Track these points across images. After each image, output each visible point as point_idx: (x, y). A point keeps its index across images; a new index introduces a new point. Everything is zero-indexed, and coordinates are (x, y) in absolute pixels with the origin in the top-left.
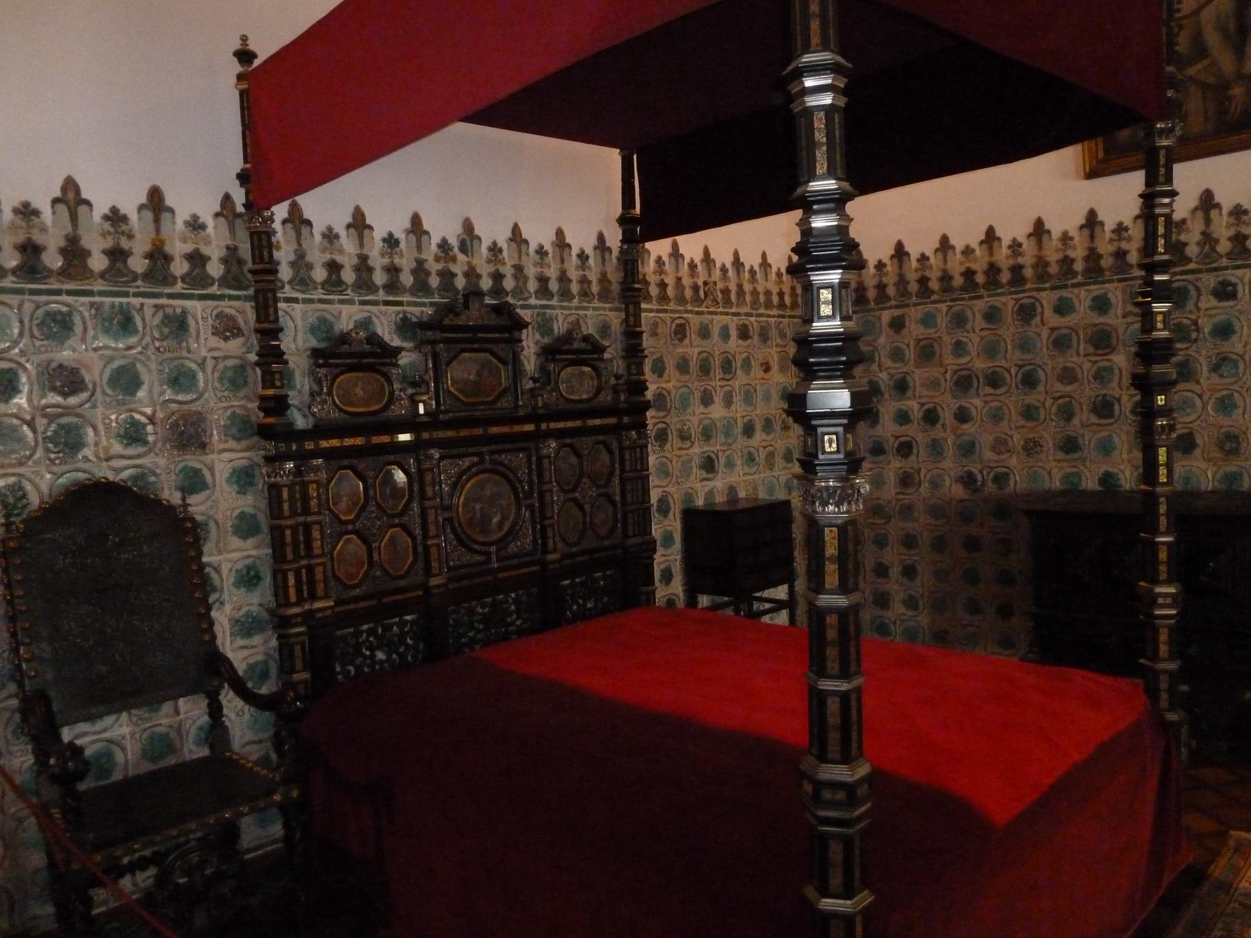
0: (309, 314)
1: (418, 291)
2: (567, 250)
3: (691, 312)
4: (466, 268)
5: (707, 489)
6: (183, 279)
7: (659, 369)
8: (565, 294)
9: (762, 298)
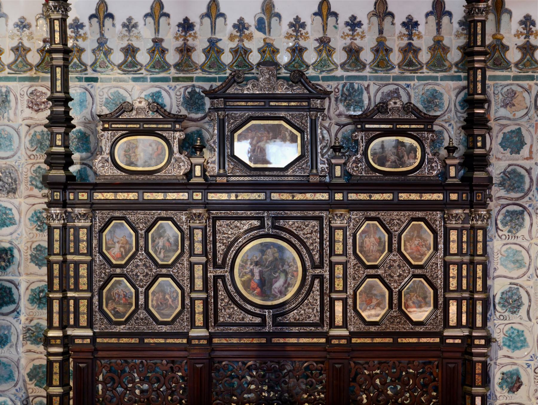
0: (105, 90)
1: (210, 67)
2: (388, 19)
4: (262, 44)
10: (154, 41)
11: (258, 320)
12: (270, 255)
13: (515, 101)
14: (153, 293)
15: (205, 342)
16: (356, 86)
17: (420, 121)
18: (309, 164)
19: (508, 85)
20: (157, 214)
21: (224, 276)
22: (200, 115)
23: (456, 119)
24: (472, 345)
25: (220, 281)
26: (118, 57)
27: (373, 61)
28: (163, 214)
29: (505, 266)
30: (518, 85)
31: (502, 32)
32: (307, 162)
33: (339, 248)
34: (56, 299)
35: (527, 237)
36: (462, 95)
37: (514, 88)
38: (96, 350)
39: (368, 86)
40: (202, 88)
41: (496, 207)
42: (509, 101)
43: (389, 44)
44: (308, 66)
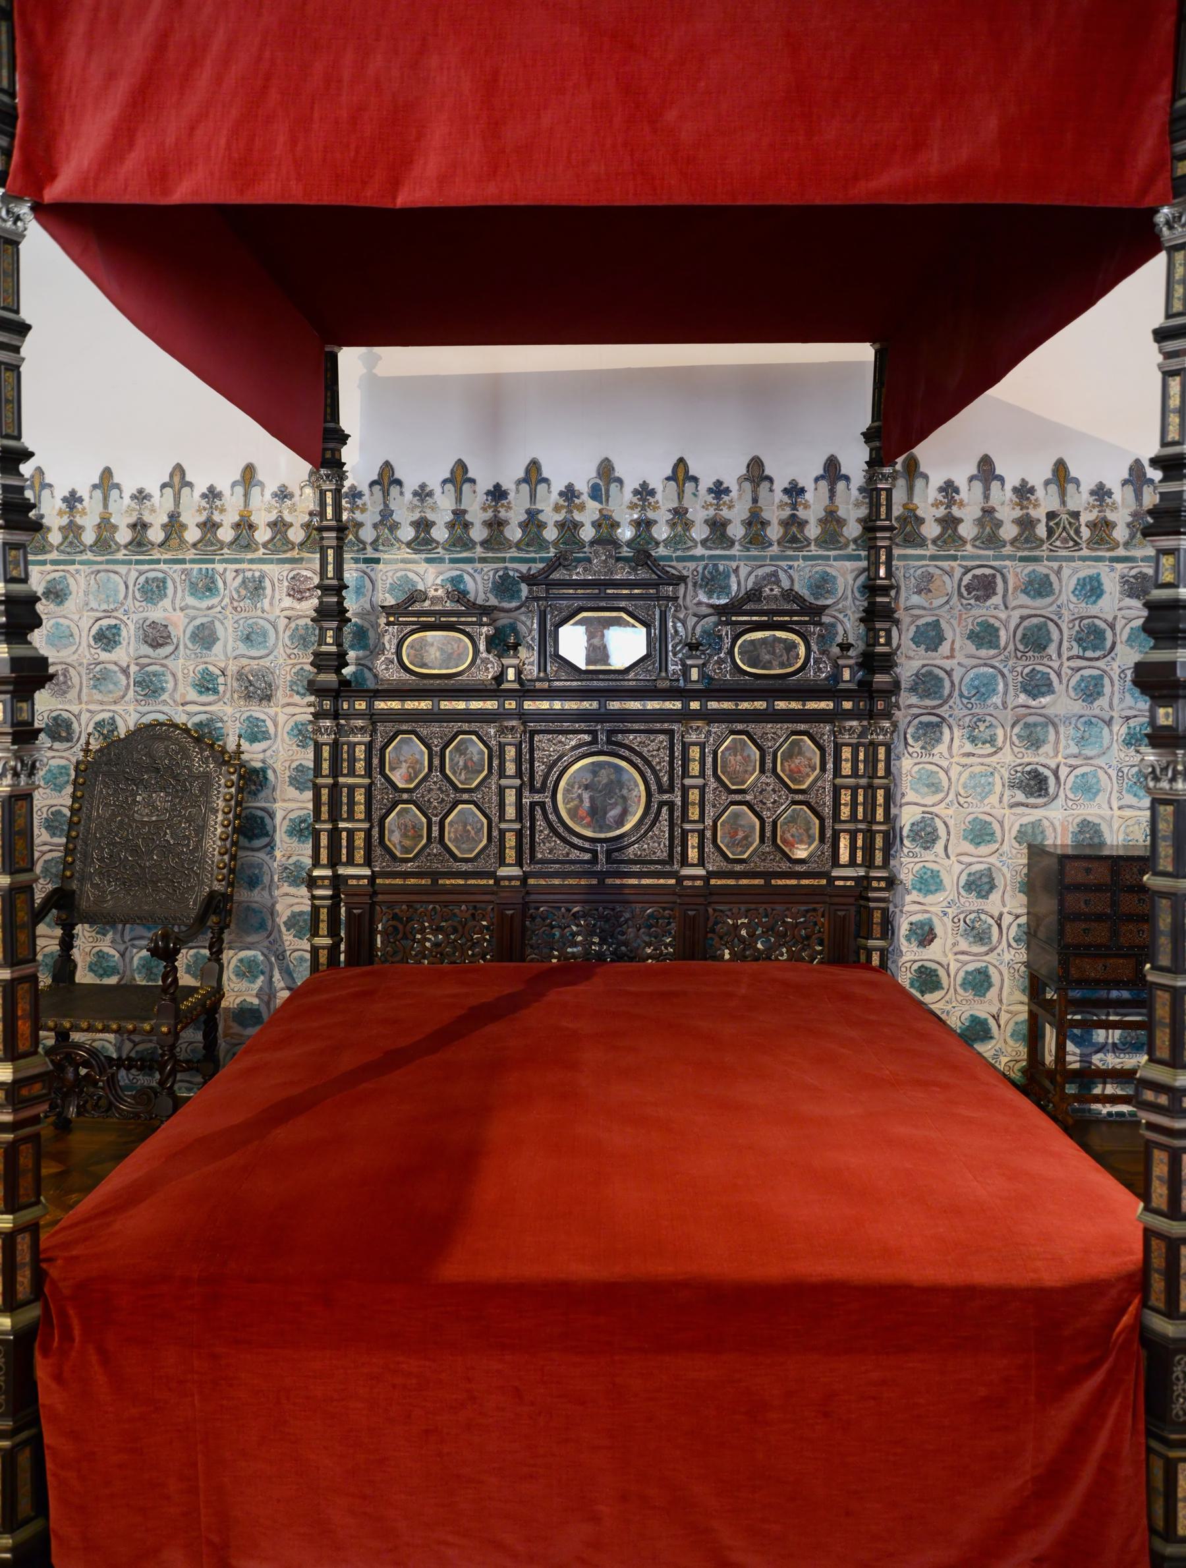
1: (528, 545)
2: (765, 485)
3: (1010, 558)
4: (596, 516)
6: (265, 546)
7: (931, 637)
10: (454, 512)
11: (587, 856)
12: (604, 777)
13: (931, 586)
14: (451, 823)
15: (518, 883)
16: (721, 568)
17: (805, 613)
18: (657, 665)
19: (923, 566)
20: (456, 726)
21: (544, 803)
22: (514, 604)
23: (854, 609)
24: (869, 888)
25: (538, 808)
27: (744, 537)
28: (465, 726)
30: (937, 567)
31: (916, 500)
32: (654, 663)
33: (694, 768)
34: (324, 830)
36: (862, 578)
37: (931, 570)
38: (375, 893)
39: (738, 567)
40: (517, 571)
41: (905, 717)
42: (925, 586)
43: (765, 515)
44: (657, 544)
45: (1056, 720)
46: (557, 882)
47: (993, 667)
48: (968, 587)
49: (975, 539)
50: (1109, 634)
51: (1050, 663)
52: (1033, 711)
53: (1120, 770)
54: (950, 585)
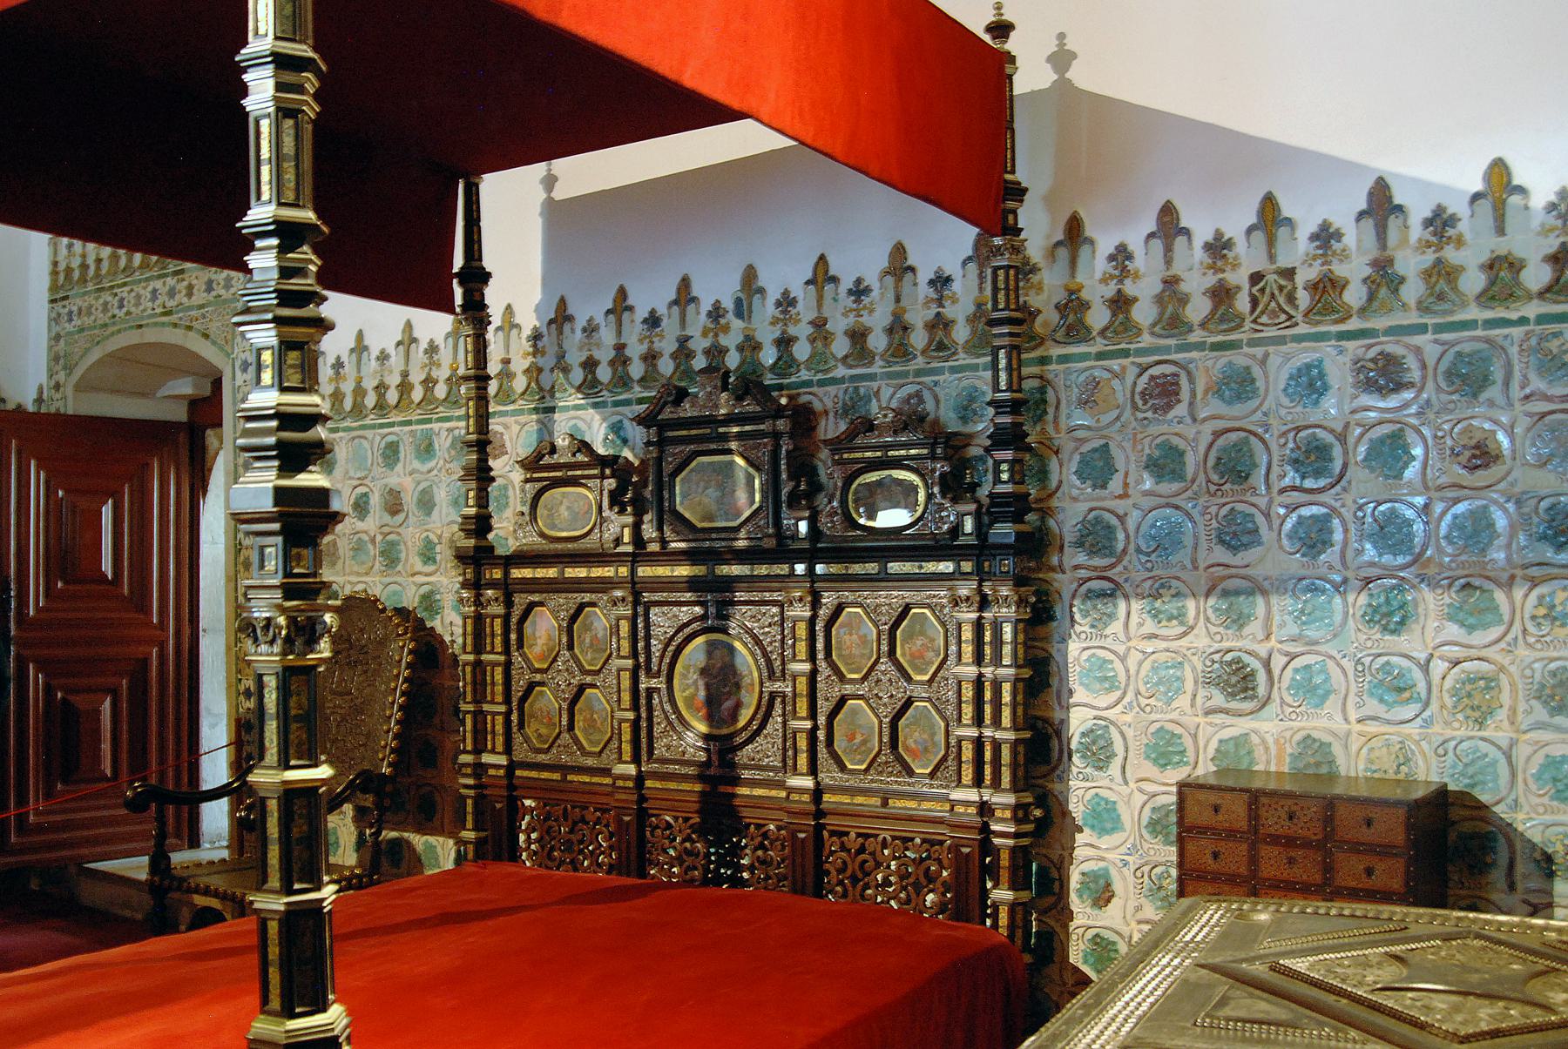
3: (1200, 346)
4: (741, 338)
5: (1226, 734)
7: (1098, 468)
8: (901, 351)
9: (1473, 281)
16: (862, 391)
26: (578, 375)
29: (1087, 686)
31: (1080, 278)
35: (1122, 636)
43: (909, 317)
45: (1266, 584)
46: (673, 785)
47: (1177, 507)
48: (1143, 393)
49: (1154, 325)
50: (1337, 451)
51: (1253, 500)
52: (1234, 571)
53: (1359, 662)
54: (1121, 391)
